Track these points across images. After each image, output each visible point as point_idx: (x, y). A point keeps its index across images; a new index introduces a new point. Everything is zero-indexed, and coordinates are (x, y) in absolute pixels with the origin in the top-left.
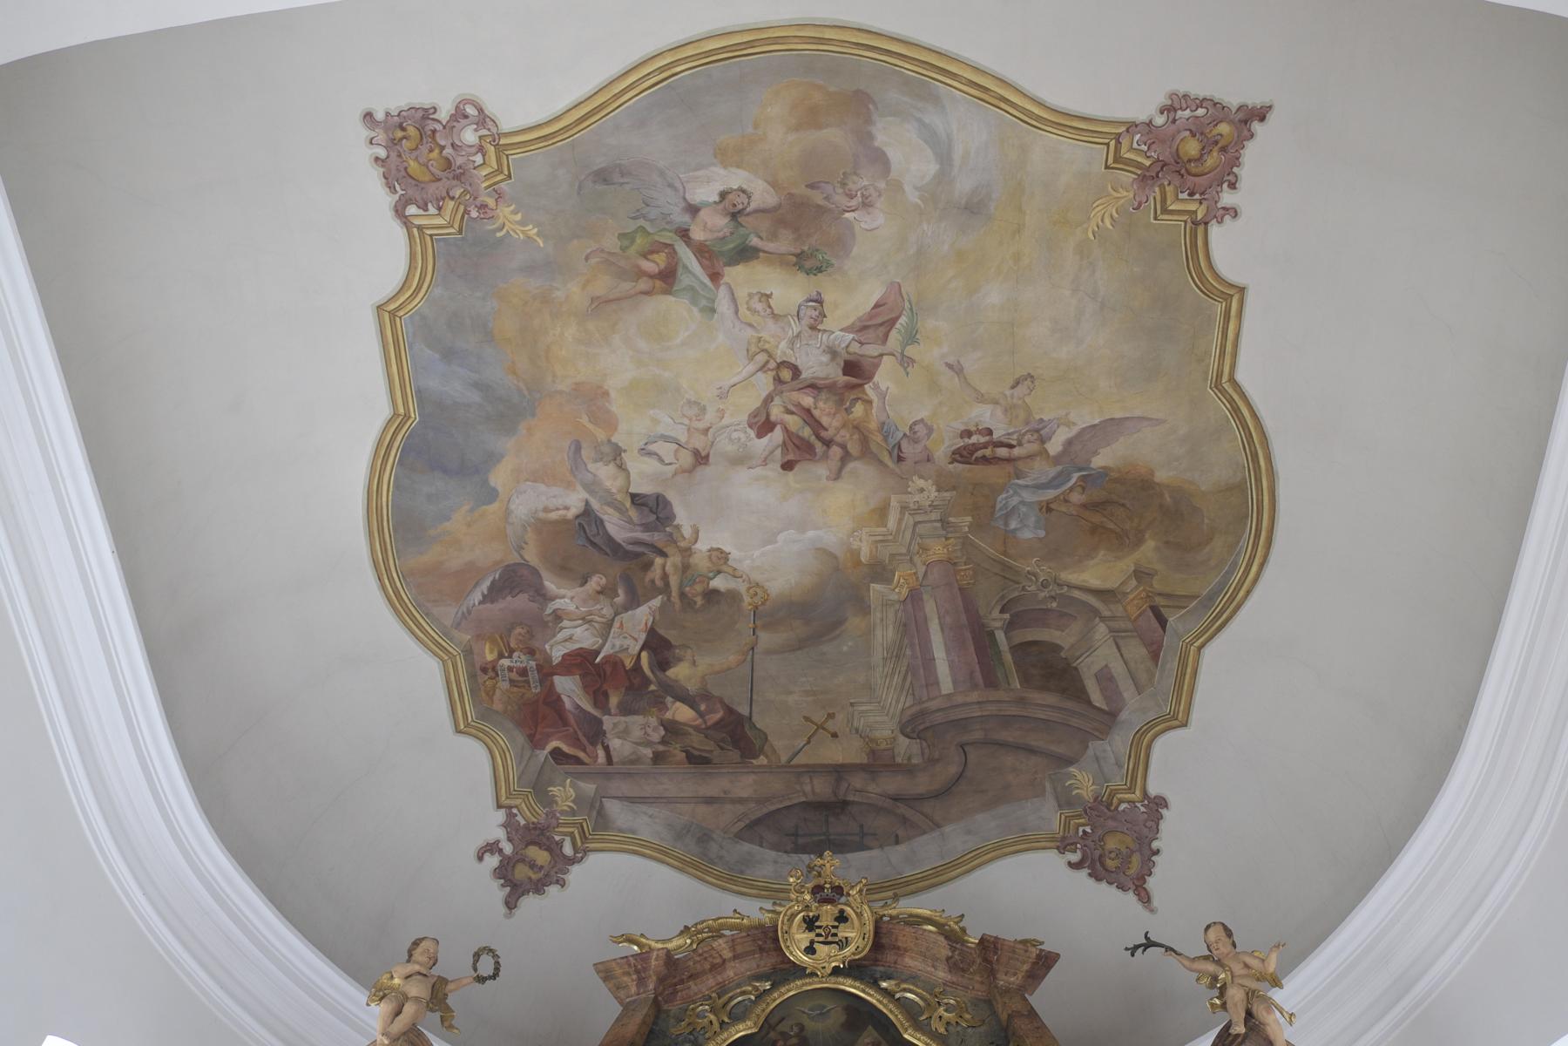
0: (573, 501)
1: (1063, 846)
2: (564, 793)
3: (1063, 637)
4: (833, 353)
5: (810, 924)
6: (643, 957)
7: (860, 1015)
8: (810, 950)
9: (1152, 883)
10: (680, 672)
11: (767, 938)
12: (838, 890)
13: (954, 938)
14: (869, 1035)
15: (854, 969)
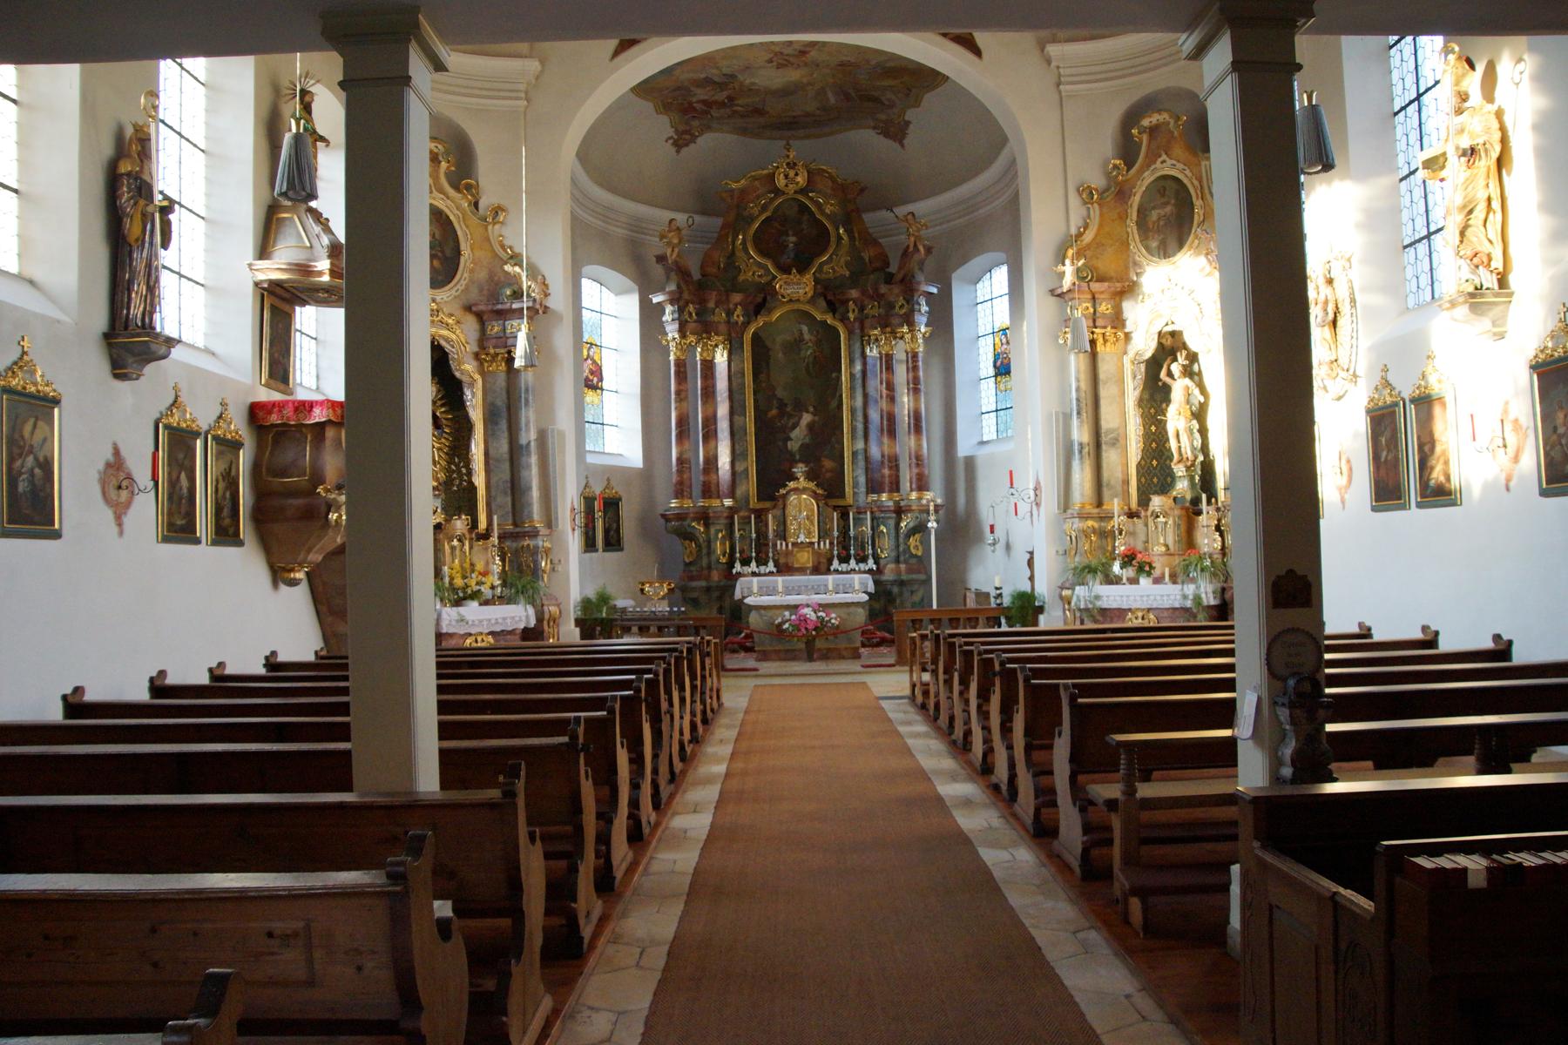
0: (703, 76)
1: (874, 128)
2: (695, 123)
3: (875, 94)
4: (795, 50)
5: (786, 176)
6: (732, 191)
7: (803, 208)
8: (786, 186)
9: (906, 142)
10: (740, 102)
11: (771, 177)
12: (795, 164)
13: (831, 177)
14: (805, 218)
15: (803, 191)
